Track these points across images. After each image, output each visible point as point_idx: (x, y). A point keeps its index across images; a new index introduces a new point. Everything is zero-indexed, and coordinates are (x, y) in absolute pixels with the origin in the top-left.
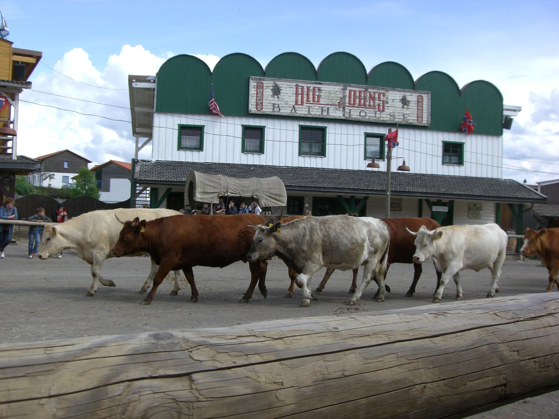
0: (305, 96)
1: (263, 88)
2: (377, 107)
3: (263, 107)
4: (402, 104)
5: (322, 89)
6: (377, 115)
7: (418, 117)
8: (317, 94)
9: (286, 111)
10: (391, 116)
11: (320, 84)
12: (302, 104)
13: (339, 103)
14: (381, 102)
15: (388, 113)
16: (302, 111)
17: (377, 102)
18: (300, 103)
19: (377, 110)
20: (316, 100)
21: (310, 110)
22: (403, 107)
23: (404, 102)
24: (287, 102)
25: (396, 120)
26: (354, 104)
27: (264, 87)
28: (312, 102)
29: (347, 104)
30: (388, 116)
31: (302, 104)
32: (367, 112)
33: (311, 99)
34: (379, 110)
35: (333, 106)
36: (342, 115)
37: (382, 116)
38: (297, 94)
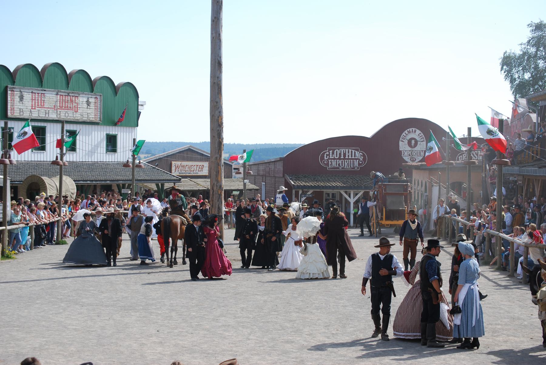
0: (37, 101)
1: (14, 95)
2: (74, 108)
3: (15, 112)
4: (87, 104)
5: (45, 95)
6: (75, 116)
7: (95, 115)
8: (43, 99)
9: (26, 115)
10: (81, 115)
11: (45, 90)
12: (35, 109)
13: (54, 106)
14: (76, 104)
15: (80, 113)
16: (35, 115)
17: (74, 104)
18: (34, 108)
19: (74, 111)
20: (42, 104)
21: (40, 113)
22: (87, 108)
23: (88, 103)
24: (27, 106)
25: (84, 118)
26: (62, 106)
27: (15, 95)
28: (40, 106)
29: (59, 107)
30: (80, 116)
31: (35, 109)
32: (69, 113)
33: (40, 104)
34: (75, 112)
35: (51, 109)
36: (56, 116)
37: (77, 115)
38: (32, 100)
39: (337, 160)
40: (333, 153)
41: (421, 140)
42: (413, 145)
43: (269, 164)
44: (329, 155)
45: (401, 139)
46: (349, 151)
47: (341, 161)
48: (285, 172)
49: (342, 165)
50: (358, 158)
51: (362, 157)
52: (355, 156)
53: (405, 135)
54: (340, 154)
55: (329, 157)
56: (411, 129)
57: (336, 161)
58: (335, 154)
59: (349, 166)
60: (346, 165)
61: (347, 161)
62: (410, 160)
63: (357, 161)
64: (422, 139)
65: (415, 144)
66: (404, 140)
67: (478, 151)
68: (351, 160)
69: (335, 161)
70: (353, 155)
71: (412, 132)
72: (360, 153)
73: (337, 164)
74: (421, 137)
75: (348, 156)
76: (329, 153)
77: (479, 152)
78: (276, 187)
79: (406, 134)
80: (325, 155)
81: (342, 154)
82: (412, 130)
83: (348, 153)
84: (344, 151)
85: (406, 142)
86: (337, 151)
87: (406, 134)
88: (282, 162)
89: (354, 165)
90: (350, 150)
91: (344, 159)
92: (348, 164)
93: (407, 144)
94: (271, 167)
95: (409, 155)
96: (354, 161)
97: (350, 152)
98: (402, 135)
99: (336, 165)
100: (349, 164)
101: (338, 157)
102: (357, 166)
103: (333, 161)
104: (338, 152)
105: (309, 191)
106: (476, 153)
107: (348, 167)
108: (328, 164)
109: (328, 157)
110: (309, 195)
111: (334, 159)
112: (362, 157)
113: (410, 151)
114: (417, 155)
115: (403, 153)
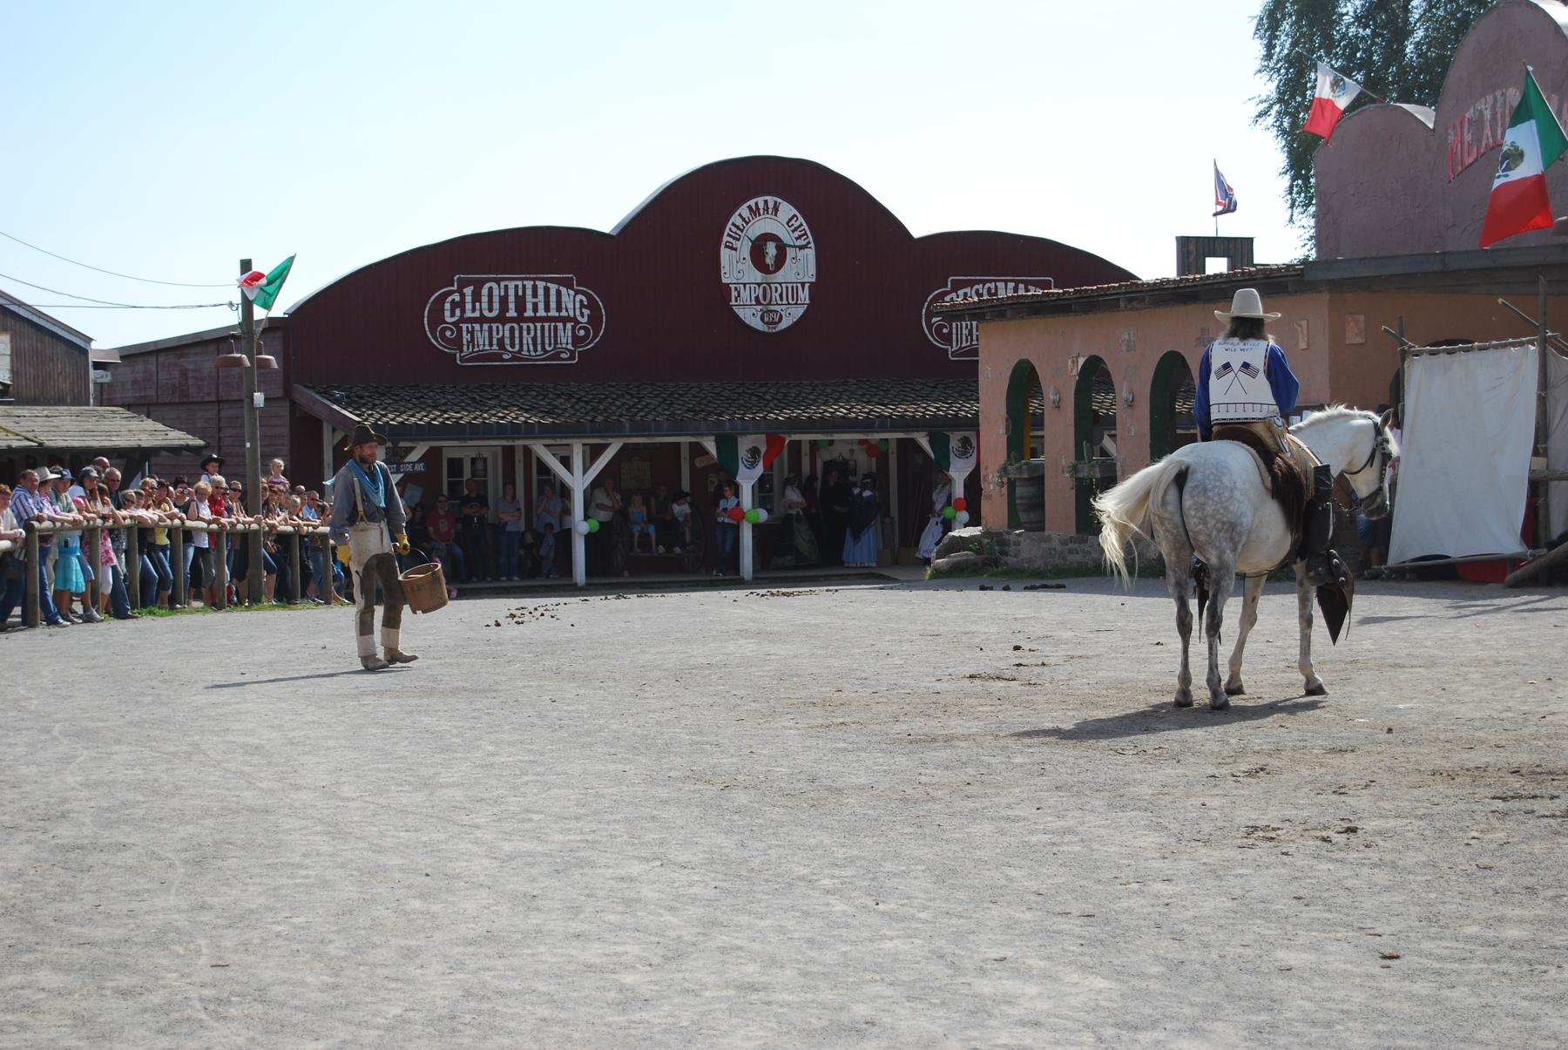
39: (494, 326)
40: (477, 297)
41: (799, 243)
42: (770, 260)
43: (182, 356)
44: (462, 304)
45: (726, 238)
46: (535, 288)
47: (507, 327)
48: (291, 372)
49: (513, 345)
50: (572, 314)
51: (586, 312)
52: (559, 309)
53: (739, 222)
54: (504, 301)
55: (463, 311)
56: (761, 200)
57: (490, 329)
58: (485, 299)
59: (539, 347)
60: (527, 344)
61: (532, 326)
62: (762, 318)
63: (569, 326)
64: (799, 238)
65: (776, 257)
66: (736, 244)
67: (995, 281)
68: (547, 325)
69: (486, 326)
70: (553, 305)
71: (766, 209)
72: (579, 297)
73: (495, 341)
74: (796, 229)
75: (535, 308)
76: (463, 296)
77: (1001, 285)
78: (226, 442)
79: (744, 219)
80: (447, 306)
81: (512, 298)
82: (766, 202)
83: (535, 295)
84: (516, 287)
85: (745, 248)
86: (491, 289)
87: (744, 219)
88: (279, 334)
89: (556, 343)
90: (541, 285)
91: (520, 319)
92: (534, 339)
93: (748, 258)
94: (191, 367)
95: (758, 302)
96: (556, 327)
97: (541, 292)
98: (729, 225)
99: (491, 344)
100: (539, 341)
101: (495, 313)
102: (570, 347)
103: (477, 327)
104: (496, 292)
105: (409, 450)
106: (989, 289)
107: (536, 350)
108: (457, 342)
109: (458, 312)
110: (414, 463)
111: (482, 320)
112: (586, 312)
113: (759, 284)
114: (785, 302)
115: (734, 294)
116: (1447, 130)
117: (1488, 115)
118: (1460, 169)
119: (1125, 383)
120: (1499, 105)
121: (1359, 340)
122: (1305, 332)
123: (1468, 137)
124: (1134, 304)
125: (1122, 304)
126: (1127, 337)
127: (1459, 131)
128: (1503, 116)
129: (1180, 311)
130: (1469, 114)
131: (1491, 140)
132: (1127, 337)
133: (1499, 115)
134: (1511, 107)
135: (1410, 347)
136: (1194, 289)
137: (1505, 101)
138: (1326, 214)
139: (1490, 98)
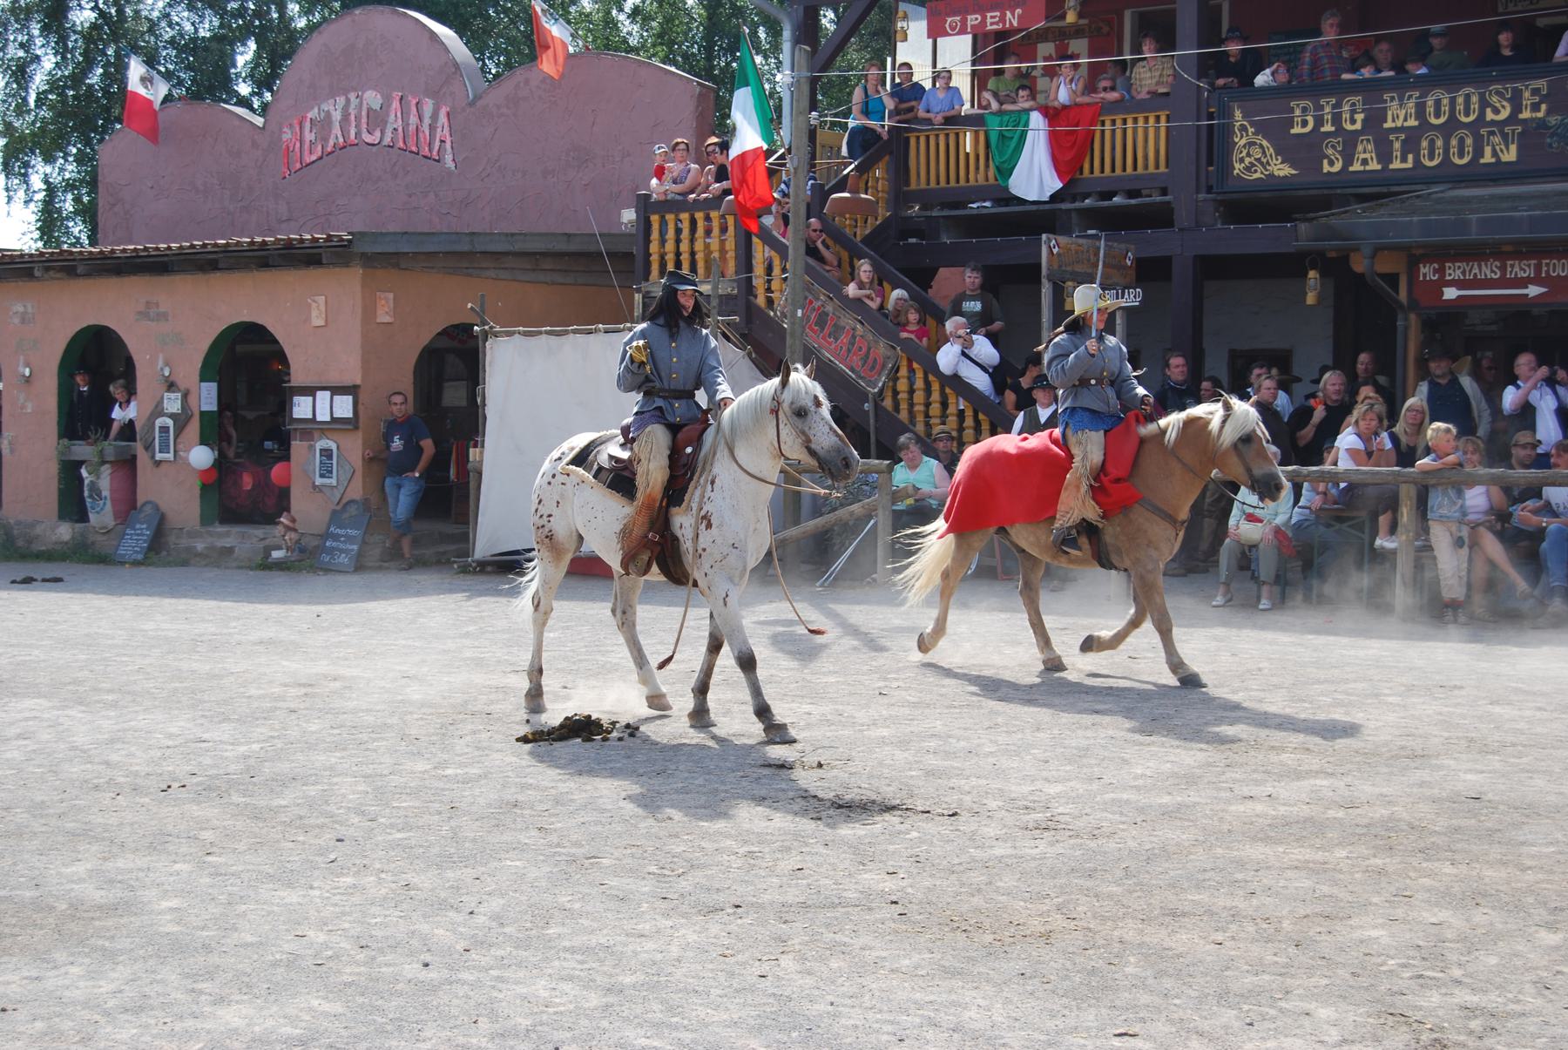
116: (281, 132)
117: (337, 116)
118: (298, 166)
119: (22, 358)
120: (352, 106)
121: (387, 319)
122: (323, 308)
123: (309, 136)
124: (51, 273)
125: (37, 273)
126: (21, 309)
127: (298, 129)
128: (358, 118)
129: (114, 282)
130: (313, 114)
131: (341, 140)
132: (21, 309)
133: (353, 117)
134: (369, 110)
135: (491, 328)
136: (166, 259)
137: (361, 104)
138: (114, 205)
139: (341, 101)
